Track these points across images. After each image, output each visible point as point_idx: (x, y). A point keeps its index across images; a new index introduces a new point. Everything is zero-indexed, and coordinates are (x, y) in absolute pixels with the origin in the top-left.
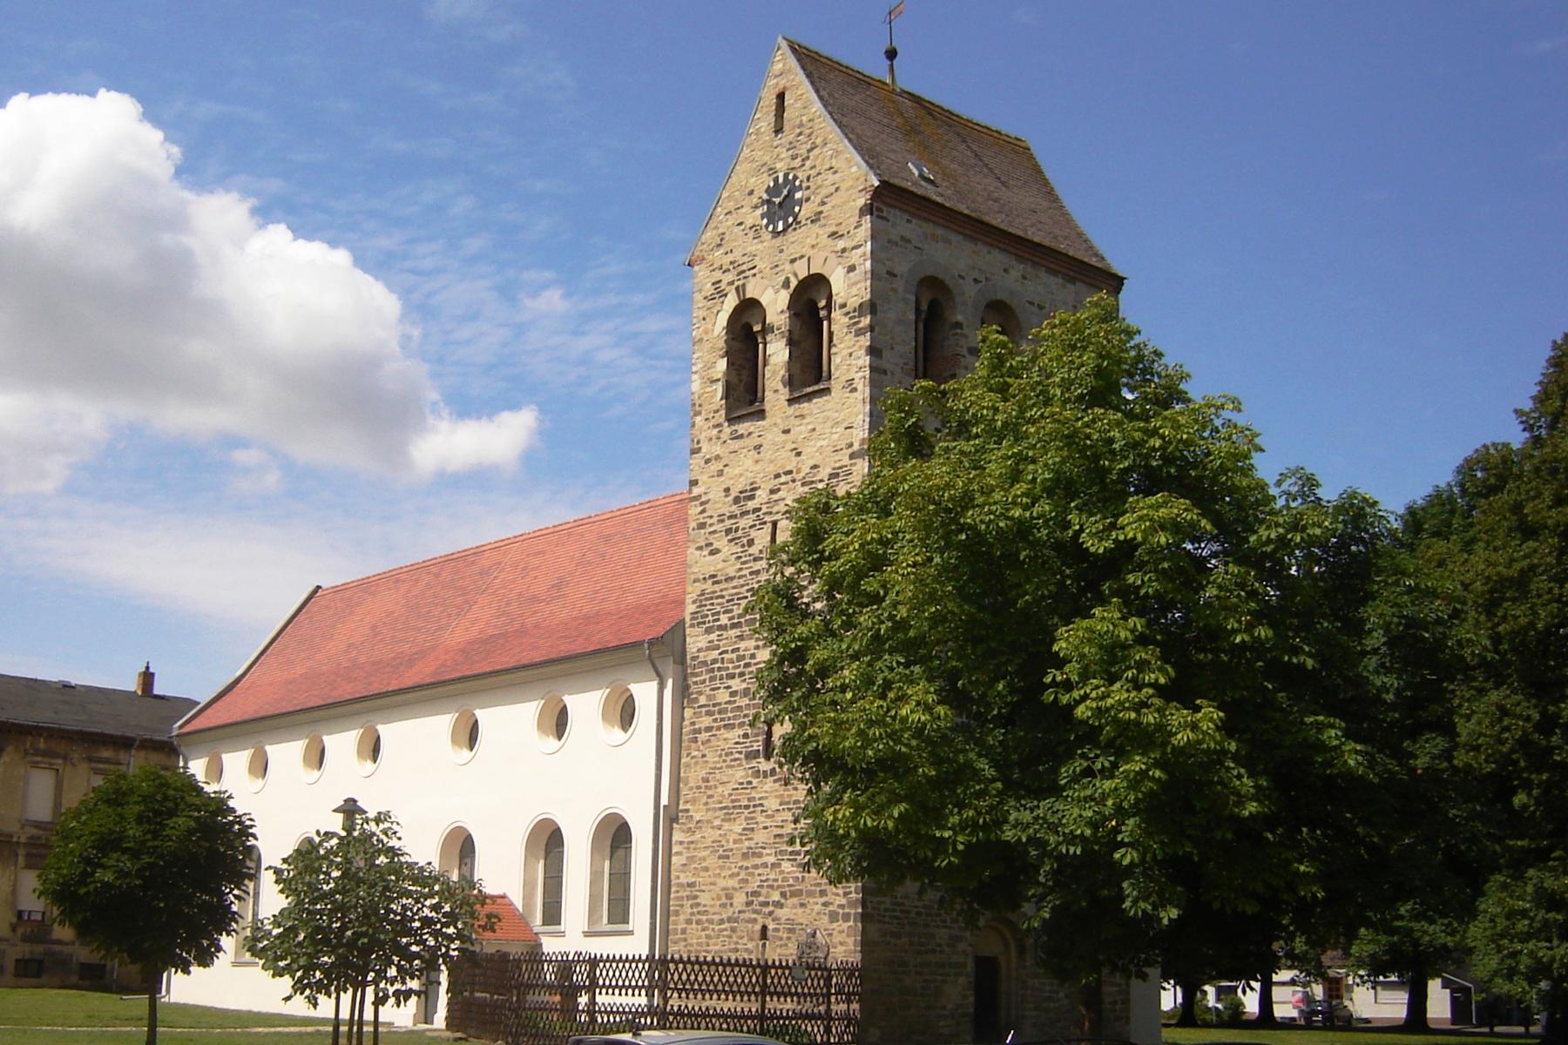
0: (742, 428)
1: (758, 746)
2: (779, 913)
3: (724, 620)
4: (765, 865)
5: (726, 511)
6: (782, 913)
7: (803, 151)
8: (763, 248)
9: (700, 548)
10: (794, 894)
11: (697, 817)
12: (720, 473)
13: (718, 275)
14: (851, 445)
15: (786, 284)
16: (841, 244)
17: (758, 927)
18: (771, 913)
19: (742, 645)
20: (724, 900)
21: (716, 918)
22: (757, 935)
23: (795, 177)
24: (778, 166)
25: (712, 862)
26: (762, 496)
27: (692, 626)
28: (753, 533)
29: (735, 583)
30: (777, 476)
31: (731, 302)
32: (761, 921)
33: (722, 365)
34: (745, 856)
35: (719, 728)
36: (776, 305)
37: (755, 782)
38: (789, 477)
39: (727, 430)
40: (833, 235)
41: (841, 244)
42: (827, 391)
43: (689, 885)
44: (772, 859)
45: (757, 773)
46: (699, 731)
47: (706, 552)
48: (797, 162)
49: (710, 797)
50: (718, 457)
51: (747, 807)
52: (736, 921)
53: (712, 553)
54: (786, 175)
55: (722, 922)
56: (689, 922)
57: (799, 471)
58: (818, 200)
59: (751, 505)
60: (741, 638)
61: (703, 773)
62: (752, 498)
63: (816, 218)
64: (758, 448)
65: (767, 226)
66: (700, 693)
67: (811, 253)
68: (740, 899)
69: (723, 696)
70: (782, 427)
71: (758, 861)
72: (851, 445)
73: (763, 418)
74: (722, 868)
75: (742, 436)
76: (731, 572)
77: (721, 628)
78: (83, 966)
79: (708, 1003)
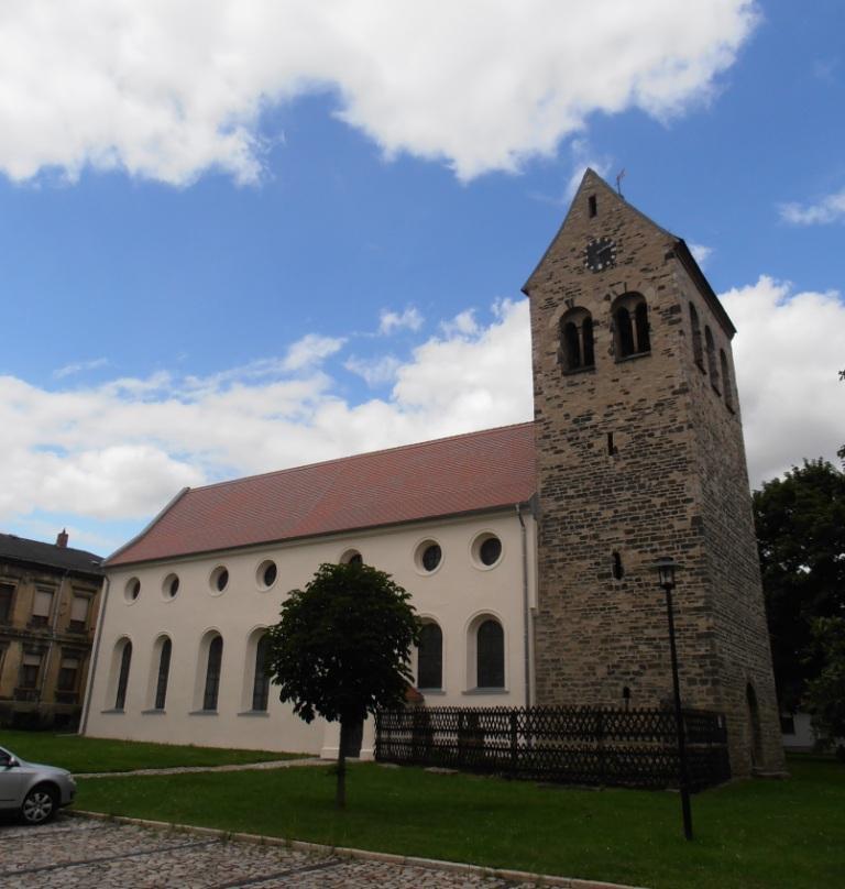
0: (578, 378)
1: (610, 569)
2: (638, 679)
3: (571, 492)
4: (624, 647)
5: (567, 427)
6: (643, 679)
7: (615, 226)
8: (587, 280)
9: (547, 450)
10: (651, 666)
11: (557, 616)
12: (560, 406)
13: (549, 295)
14: (673, 387)
15: (608, 298)
16: (651, 275)
17: (620, 689)
18: (631, 679)
19: (588, 508)
20: (587, 670)
21: (581, 683)
22: (621, 695)
23: (610, 241)
24: (595, 235)
25: (573, 645)
26: (597, 418)
27: (543, 497)
28: (592, 440)
29: (578, 470)
30: (610, 406)
31: (562, 309)
32: (622, 684)
33: (556, 345)
34: (604, 641)
35: (571, 560)
36: (600, 310)
37: (609, 593)
38: (620, 407)
39: (564, 381)
40: (644, 270)
41: (651, 275)
42: (649, 355)
43: (553, 661)
44: (629, 643)
45: (610, 588)
46: (555, 561)
47: (551, 452)
48: (611, 232)
49: (567, 603)
50: (557, 397)
51: (601, 610)
52: (600, 684)
53: (557, 453)
54: (602, 239)
55: (586, 685)
56: (555, 685)
57: (628, 403)
58: (629, 252)
59: (588, 424)
60: (587, 503)
61: (561, 588)
62: (590, 419)
63: (629, 261)
64: (592, 391)
65: (589, 267)
66: (554, 538)
67: (627, 280)
68: (601, 671)
69: (574, 539)
70: (611, 378)
71: (616, 645)
72: (673, 387)
73: (594, 373)
74: (583, 650)
75: (577, 384)
76: (576, 464)
77: (567, 497)
78: (696, 684)
79: (573, 742)
